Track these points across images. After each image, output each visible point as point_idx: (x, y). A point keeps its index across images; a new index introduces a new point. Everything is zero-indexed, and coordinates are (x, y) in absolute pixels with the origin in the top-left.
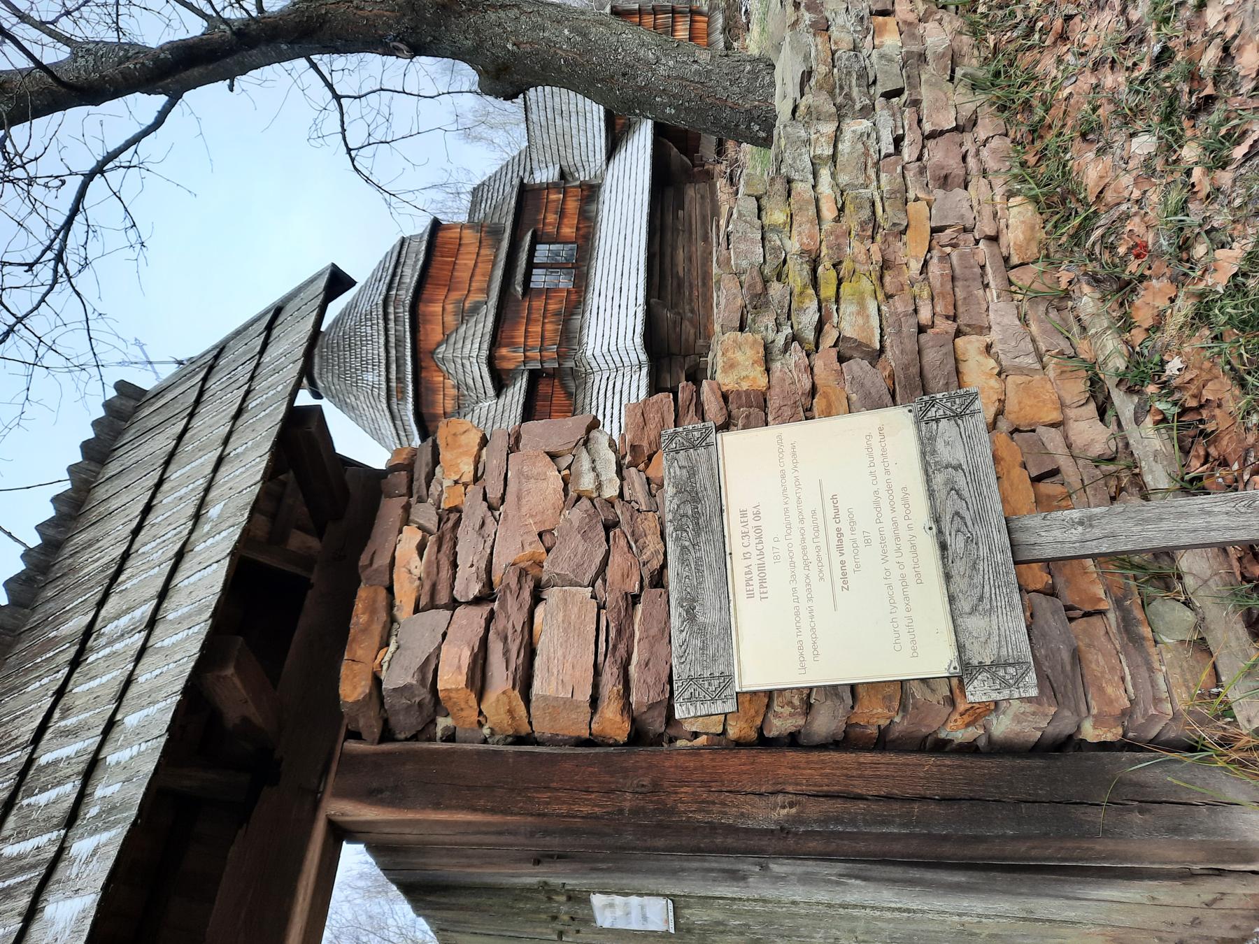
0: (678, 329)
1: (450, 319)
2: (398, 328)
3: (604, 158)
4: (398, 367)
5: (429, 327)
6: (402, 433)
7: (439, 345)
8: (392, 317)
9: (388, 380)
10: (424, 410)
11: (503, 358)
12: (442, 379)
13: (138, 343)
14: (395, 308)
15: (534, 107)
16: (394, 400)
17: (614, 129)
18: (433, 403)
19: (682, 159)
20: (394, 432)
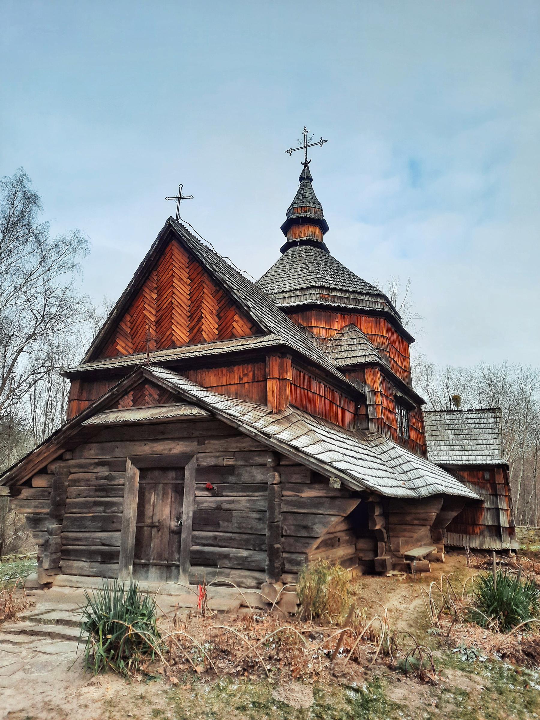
1: (379, 340)
3: (442, 462)
4: (342, 298)
6: (287, 295)
8: (375, 300)
9: (333, 289)
12: (337, 329)
13: (322, 142)
14: (381, 303)
15: (453, 417)
16: (320, 292)
17: (460, 470)
19: (449, 520)
20: (287, 289)
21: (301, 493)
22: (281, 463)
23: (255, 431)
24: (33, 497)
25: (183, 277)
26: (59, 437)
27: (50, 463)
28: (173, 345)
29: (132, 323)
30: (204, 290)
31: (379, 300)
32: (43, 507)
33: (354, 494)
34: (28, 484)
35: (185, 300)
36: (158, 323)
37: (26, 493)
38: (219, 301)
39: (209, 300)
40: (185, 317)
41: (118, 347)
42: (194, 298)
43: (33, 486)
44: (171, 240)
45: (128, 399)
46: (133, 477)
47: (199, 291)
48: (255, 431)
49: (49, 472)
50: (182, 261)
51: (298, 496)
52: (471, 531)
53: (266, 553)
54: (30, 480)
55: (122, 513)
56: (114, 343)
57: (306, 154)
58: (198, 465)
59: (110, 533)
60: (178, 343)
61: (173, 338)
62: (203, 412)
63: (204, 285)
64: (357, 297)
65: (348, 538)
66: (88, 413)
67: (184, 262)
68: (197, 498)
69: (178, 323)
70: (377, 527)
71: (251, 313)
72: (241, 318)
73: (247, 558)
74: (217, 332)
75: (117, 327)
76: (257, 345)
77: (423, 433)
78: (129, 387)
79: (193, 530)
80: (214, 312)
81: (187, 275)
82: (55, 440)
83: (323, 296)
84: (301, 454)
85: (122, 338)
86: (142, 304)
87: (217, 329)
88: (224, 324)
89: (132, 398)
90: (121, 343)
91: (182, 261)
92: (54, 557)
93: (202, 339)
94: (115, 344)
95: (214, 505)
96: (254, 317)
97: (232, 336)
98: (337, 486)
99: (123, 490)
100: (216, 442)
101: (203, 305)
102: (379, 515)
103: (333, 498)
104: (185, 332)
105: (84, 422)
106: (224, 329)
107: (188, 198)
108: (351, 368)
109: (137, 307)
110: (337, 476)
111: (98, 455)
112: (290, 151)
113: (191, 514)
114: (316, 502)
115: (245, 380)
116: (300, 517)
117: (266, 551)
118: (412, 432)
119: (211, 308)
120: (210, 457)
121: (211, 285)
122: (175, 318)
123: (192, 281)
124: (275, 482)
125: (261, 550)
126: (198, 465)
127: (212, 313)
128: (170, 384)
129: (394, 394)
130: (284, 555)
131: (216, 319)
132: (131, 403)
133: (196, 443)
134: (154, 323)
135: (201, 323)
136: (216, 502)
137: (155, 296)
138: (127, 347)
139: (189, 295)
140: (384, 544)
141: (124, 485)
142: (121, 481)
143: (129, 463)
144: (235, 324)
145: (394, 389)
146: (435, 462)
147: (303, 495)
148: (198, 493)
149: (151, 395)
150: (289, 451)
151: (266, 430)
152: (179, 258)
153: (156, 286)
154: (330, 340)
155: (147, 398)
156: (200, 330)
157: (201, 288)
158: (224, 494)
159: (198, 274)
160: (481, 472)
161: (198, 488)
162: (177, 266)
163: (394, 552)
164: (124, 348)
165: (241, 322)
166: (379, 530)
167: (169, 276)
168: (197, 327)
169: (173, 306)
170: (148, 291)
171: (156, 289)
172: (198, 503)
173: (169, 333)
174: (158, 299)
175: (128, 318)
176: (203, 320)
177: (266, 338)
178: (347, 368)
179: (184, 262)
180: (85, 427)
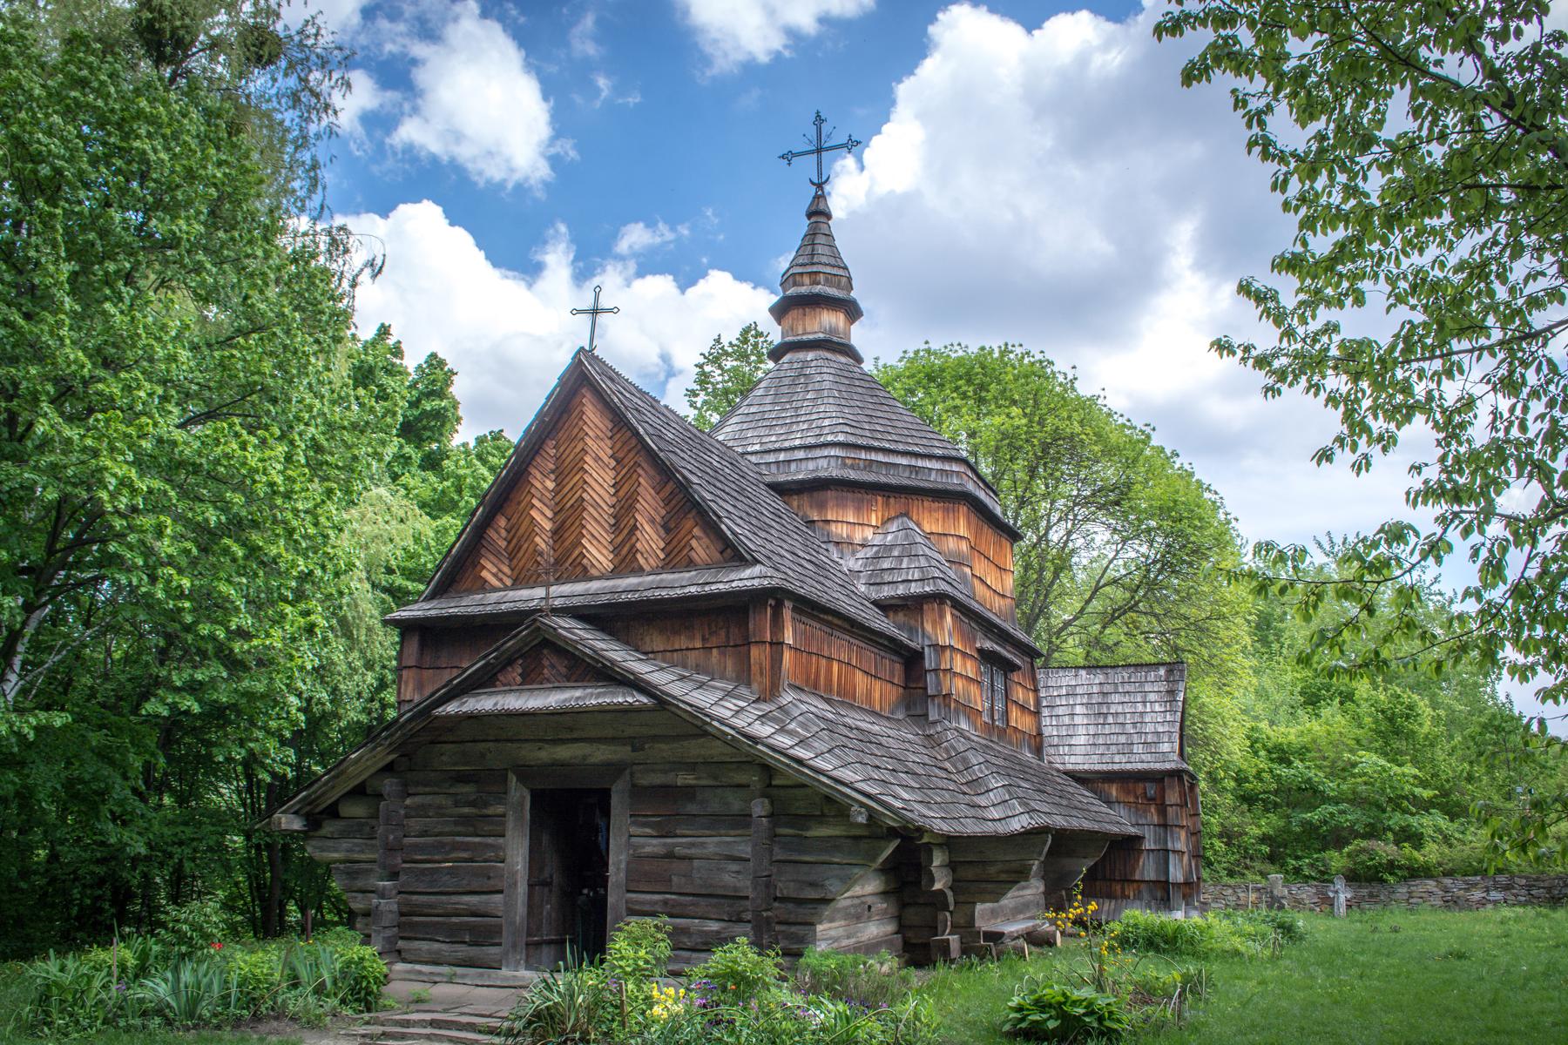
0: (1004, 877)
2: (934, 473)
3: (1070, 767)
5: (940, 515)
6: (782, 456)
7: (918, 525)
10: (829, 494)
11: (942, 616)
12: (874, 523)
18: (841, 505)
21: (808, 829)
22: (774, 783)
23: (732, 732)
24: (345, 835)
25: (601, 454)
26: (392, 735)
27: (371, 776)
28: (585, 576)
29: (508, 532)
30: (641, 480)
31: (955, 468)
32: (362, 852)
33: (892, 833)
34: (333, 812)
35: (607, 497)
36: (555, 532)
37: (329, 828)
38: (667, 502)
39: (649, 498)
40: (606, 526)
41: (484, 574)
42: (621, 493)
43: (342, 815)
44: (581, 386)
45: (515, 673)
46: (522, 805)
47: (631, 481)
48: (732, 732)
49: (369, 791)
50: (601, 425)
51: (801, 836)
52: (1119, 893)
53: (750, 925)
54: (336, 804)
55: (503, 862)
56: (476, 565)
57: (819, 163)
58: (634, 786)
59: (484, 897)
60: (594, 572)
61: (585, 561)
62: (645, 700)
63: (640, 471)
64: (913, 462)
65: (885, 905)
66: (445, 694)
67: (604, 429)
68: (633, 839)
69: (593, 535)
70: (937, 886)
71: (723, 527)
72: (705, 532)
73: (718, 932)
74: (662, 556)
75: (481, 537)
76: (734, 585)
77: (1037, 714)
78: (515, 652)
79: (628, 891)
80: (658, 519)
81: (610, 452)
82: (386, 738)
83: (849, 462)
84: (806, 771)
85: (492, 557)
86: (529, 496)
87: (662, 550)
88: (675, 542)
89: (520, 671)
90: (489, 566)
91: (601, 425)
92: (388, 933)
93: (635, 565)
94: (479, 567)
95: (661, 851)
96: (729, 533)
97: (690, 564)
98: (862, 819)
99: (503, 824)
100: (663, 746)
101: (638, 506)
102: (941, 866)
103: (856, 838)
104: (605, 552)
105: (440, 709)
106: (676, 551)
107: (610, 311)
108: (899, 602)
109: (519, 503)
110: (862, 805)
111: (455, 764)
112: (788, 157)
113: (623, 866)
114: (831, 844)
115: (714, 641)
116: (805, 868)
117: (749, 922)
118: (1015, 713)
119: (652, 512)
120: (653, 771)
121: (652, 472)
122: (588, 526)
123: (618, 462)
124: (763, 814)
125: (740, 921)
126: (634, 786)
127: (652, 521)
128: (587, 651)
129: (978, 645)
130: (778, 928)
131: (662, 532)
132: (519, 679)
133: (629, 748)
134: (549, 534)
135: (634, 539)
136: (665, 844)
137: (550, 485)
138: (500, 575)
139: (613, 486)
140: (948, 914)
141: (504, 816)
142: (500, 809)
143: (513, 779)
144: (694, 543)
145: (979, 635)
146: (1061, 767)
147: (808, 834)
148: (633, 830)
149: (553, 666)
150: (788, 765)
151: (749, 730)
152: (596, 421)
153: (553, 467)
154: (863, 546)
155: (546, 671)
156: (633, 551)
157: (635, 476)
158: (678, 832)
159: (630, 451)
160: (1141, 785)
161: (633, 823)
162: (590, 433)
163: (966, 928)
164: (495, 575)
165: (706, 540)
166: (941, 892)
167: (577, 450)
168: (628, 546)
169: (585, 504)
170: (539, 476)
171: (553, 472)
172: (635, 847)
173: (577, 552)
174: (556, 492)
175: (502, 522)
176: (638, 533)
177: (748, 573)
178: (893, 602)
179: (604, 429)
180: (437, 717)
